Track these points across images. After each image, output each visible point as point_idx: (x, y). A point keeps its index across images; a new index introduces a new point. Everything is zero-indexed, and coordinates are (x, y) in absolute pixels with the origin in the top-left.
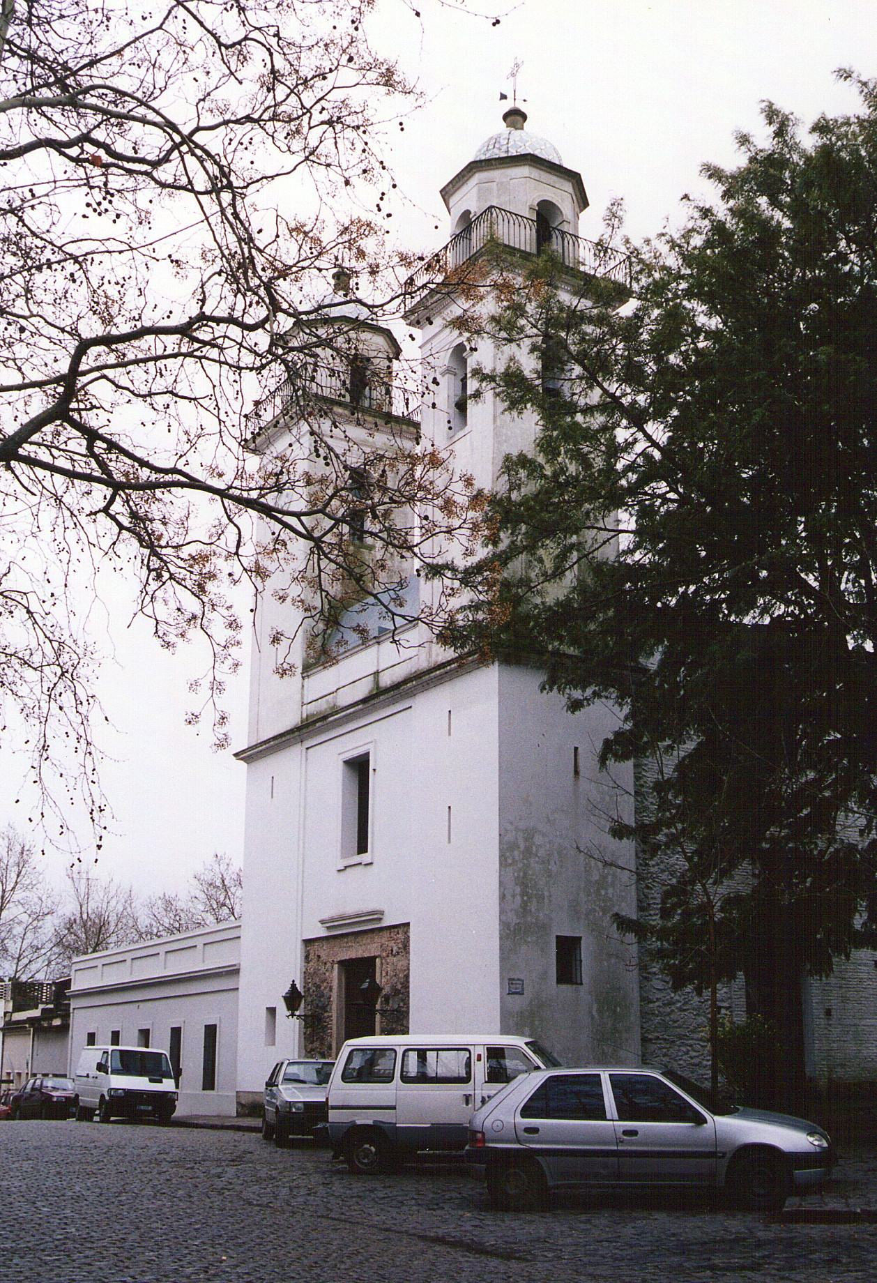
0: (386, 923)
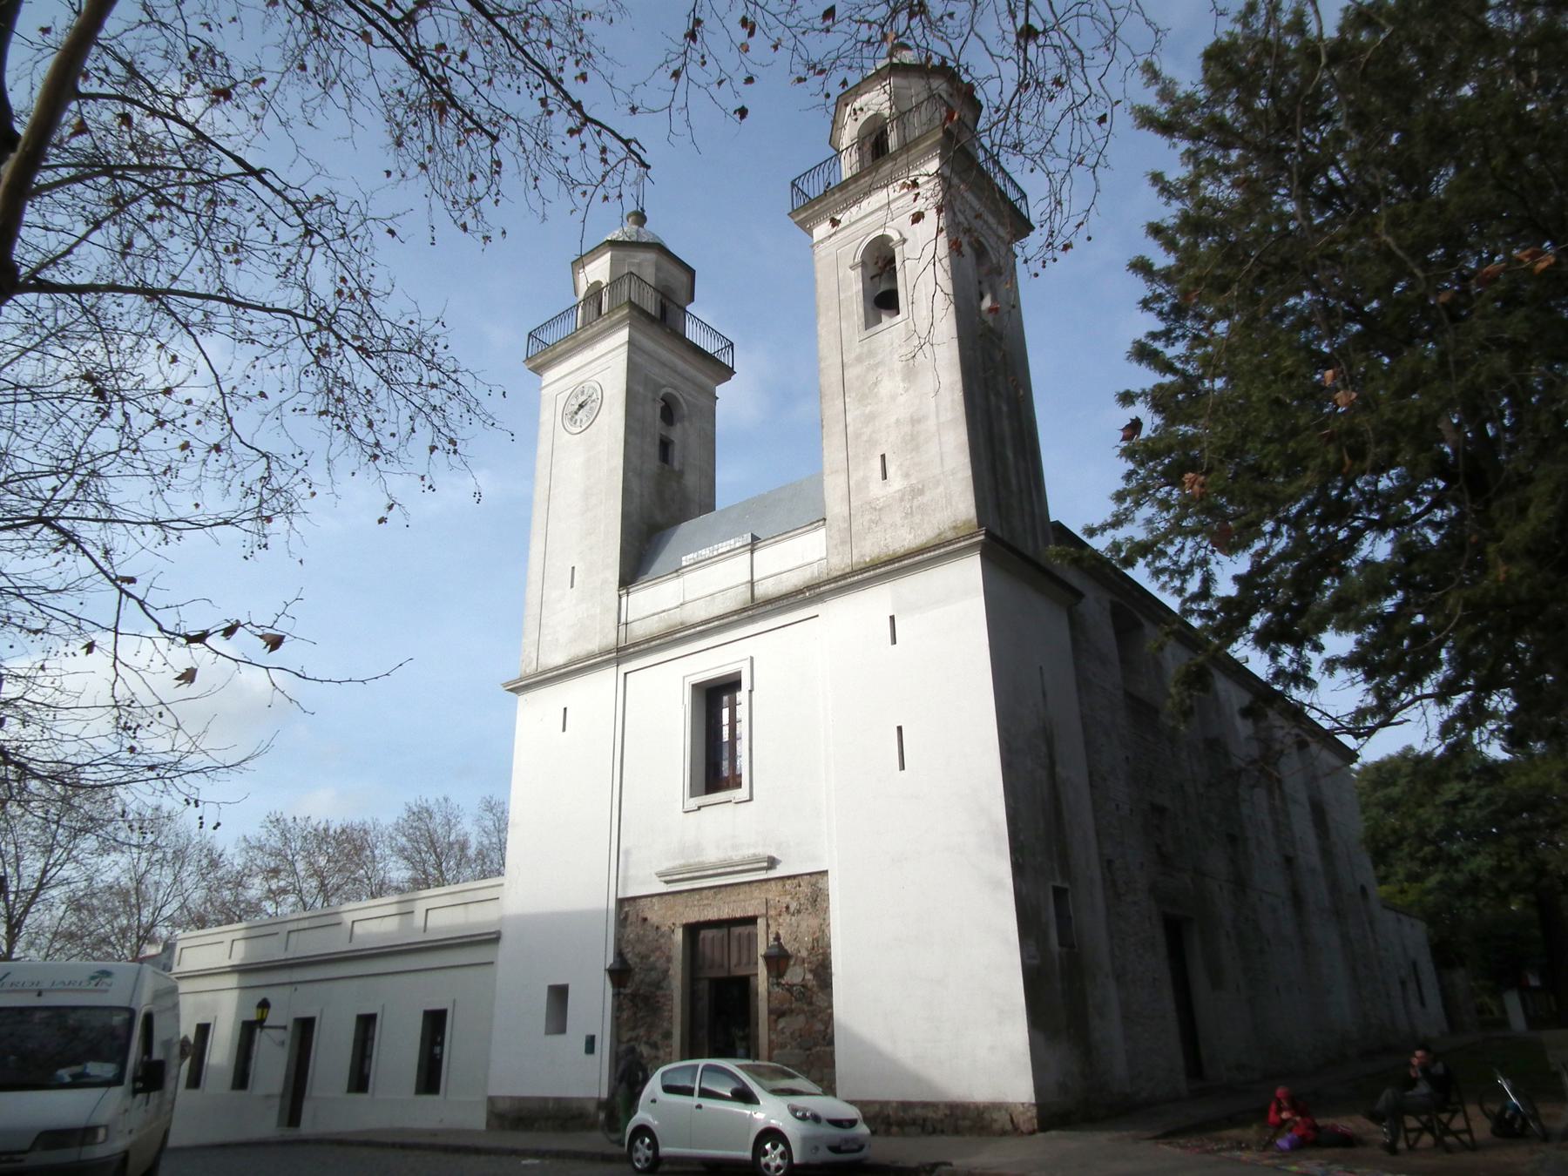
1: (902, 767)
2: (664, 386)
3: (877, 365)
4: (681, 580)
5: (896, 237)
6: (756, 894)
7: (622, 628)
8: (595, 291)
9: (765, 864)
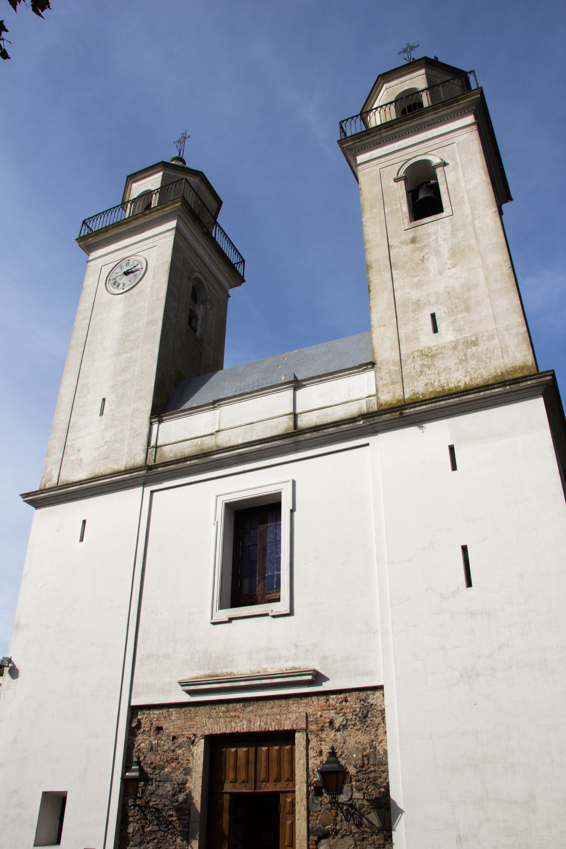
0: (326, 686)
1: (469, 584)
2: (196, 272)
3: (422, 248)
4: (217, 411)
5: (435, 160)
6: (294, 707)
7: (152, 451)
8: (148, 194)
9: (310, 677)
